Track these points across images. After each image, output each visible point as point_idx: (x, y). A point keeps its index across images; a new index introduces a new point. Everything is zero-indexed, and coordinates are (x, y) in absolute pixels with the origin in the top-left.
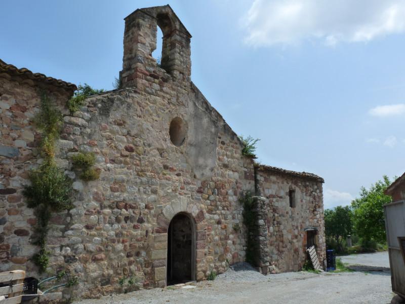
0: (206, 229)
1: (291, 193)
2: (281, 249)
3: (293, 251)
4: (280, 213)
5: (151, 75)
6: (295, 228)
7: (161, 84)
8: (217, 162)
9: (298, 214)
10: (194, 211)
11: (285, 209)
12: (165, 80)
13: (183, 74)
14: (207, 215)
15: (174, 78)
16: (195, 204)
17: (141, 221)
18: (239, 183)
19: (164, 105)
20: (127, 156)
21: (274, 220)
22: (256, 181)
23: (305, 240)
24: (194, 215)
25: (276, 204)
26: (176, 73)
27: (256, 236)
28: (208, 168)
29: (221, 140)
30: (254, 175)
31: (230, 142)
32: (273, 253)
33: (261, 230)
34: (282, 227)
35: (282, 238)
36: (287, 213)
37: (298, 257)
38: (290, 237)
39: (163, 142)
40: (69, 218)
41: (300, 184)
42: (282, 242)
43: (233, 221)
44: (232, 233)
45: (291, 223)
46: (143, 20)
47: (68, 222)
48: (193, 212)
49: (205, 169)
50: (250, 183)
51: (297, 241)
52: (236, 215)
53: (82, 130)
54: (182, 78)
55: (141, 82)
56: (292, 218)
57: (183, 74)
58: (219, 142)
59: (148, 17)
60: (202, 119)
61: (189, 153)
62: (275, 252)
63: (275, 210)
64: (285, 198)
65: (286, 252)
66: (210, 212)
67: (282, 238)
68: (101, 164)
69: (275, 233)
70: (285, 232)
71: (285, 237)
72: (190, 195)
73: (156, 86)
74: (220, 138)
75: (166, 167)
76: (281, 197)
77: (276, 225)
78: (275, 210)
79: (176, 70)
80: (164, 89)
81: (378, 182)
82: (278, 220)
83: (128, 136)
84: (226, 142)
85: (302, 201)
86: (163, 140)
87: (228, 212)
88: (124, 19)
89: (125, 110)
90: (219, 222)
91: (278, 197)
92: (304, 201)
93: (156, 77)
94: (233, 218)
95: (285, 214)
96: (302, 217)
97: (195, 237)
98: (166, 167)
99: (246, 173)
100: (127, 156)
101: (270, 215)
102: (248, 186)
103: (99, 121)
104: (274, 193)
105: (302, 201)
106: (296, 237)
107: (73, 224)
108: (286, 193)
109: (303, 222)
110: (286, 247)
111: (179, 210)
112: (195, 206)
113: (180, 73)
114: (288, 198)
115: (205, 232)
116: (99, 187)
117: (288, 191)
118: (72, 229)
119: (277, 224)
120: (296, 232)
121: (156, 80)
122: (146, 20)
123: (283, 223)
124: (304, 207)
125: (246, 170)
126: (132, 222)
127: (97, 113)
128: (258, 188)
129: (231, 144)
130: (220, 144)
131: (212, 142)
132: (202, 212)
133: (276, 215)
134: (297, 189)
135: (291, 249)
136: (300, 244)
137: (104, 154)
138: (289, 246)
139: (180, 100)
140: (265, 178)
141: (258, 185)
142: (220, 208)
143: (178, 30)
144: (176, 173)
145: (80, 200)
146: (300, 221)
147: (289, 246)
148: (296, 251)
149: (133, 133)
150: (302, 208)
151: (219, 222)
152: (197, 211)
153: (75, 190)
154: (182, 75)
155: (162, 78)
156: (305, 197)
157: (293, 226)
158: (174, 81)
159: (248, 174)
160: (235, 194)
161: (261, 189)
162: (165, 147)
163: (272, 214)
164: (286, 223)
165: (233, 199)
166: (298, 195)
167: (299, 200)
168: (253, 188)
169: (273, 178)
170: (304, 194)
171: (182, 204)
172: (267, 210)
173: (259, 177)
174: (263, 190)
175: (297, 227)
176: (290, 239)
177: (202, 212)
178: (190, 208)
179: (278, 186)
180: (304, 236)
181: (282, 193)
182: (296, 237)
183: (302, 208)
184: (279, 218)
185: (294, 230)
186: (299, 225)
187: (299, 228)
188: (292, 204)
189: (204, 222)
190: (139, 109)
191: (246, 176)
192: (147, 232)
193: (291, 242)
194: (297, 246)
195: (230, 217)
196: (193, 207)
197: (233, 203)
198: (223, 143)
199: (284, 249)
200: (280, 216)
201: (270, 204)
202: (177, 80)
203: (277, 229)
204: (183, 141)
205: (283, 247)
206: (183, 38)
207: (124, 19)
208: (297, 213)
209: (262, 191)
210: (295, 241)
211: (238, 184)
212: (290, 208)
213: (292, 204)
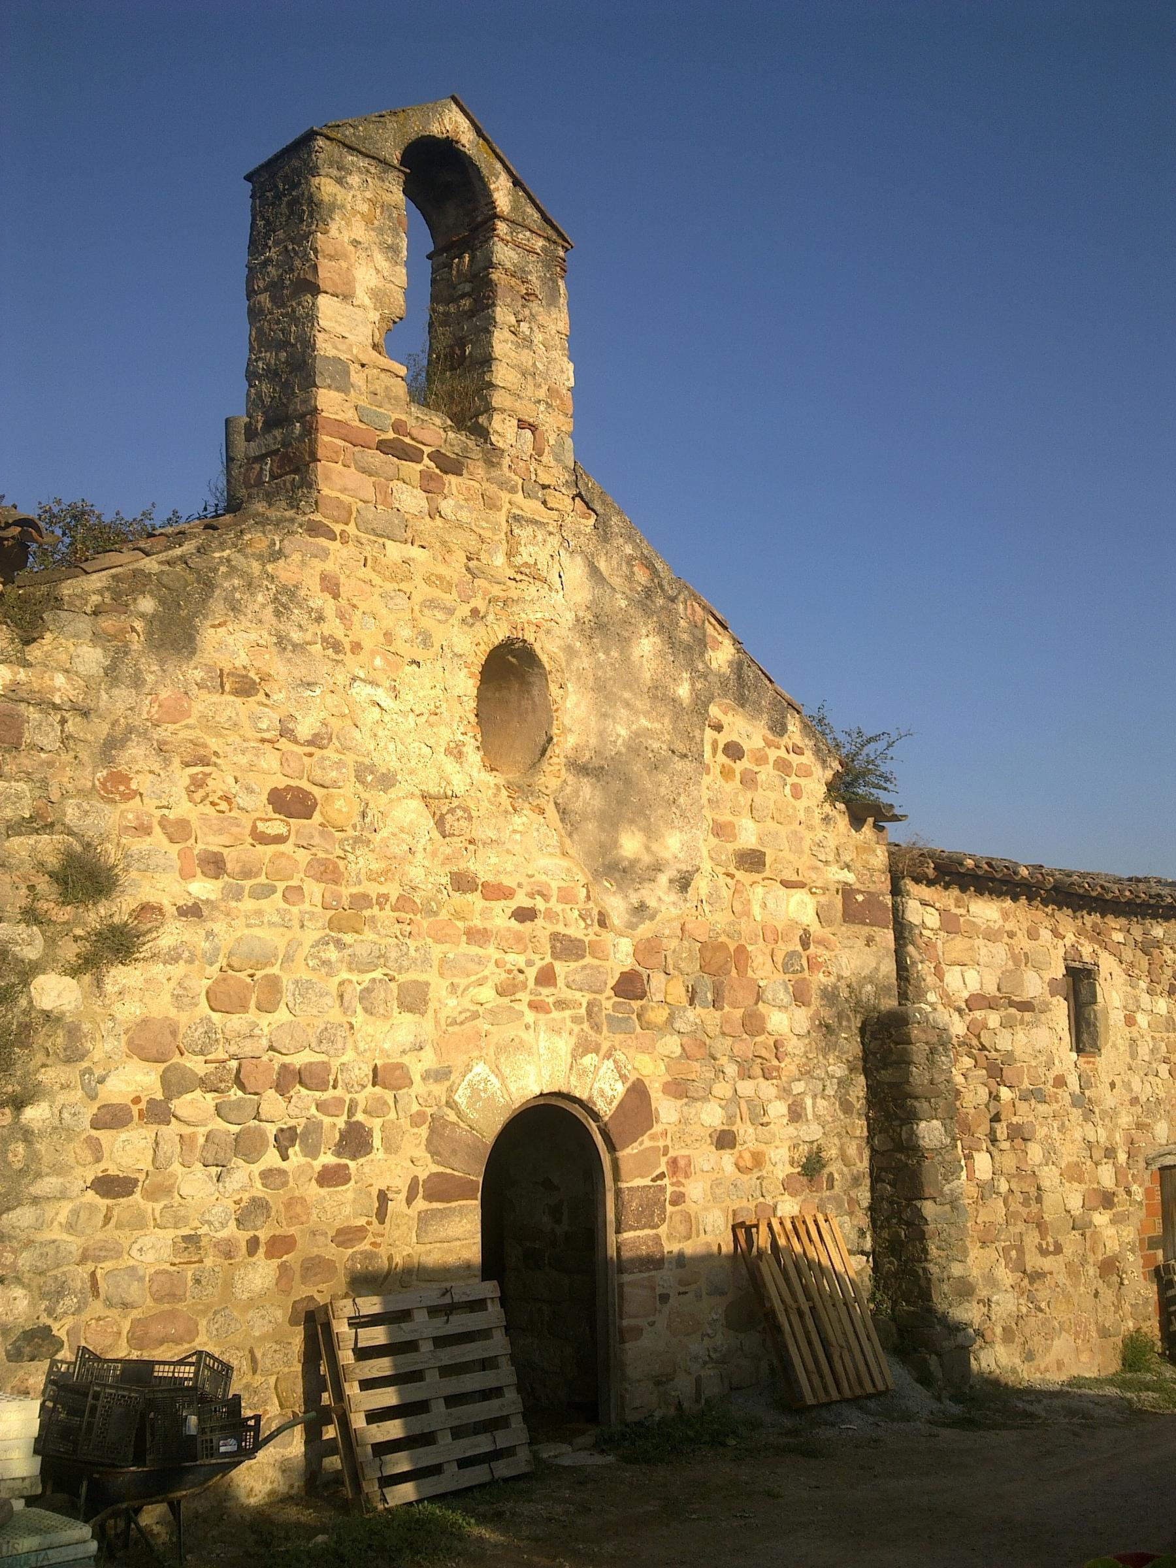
0: (662, 1176)
1: (1079, 983)
2: (1034, 1261)
3: (1092, 1271)
4: (1026, 1085)
5: (384, 447)
6: (1098, 1154)
7: (429, 484)
8: (706, 843)
9: (1113, 1085)
10: (602, 1087)
11: (1049, 1065)
12: (450, 465)
13: (533, 428)
14: (667, 1110)
15: (492, 456)
16: (608, 1056)
17: (355, 1141)
18: (820, 942)
19: (448, 587)
20: (280, 839)
21: (996, 1118)
22: (902, 931)
23: (1149, 1214)
24: (605, 1109)
25: (1004, 1041)
26: (503, 430)
27: (909, 1200)
28: (663, 879)
29: (723, 739)
30: (888, 900)
31: (769, 744)
32: (991, 1281)
33: (931, 1170)
34: (1035, 1152)
35: (1035, 1208)
36: (1060, 1082)
37: (1119, 1297)
38: (1075, 1203)
39: (450, 766)
40: (21, 1148)
41: (1118, 937)
42: (1041, 1226)
43: (791, 1130)
44: (787, 1186)
45: (1077, 1134)
46: (340, 181)
47: (18, 1166)
48: (602, 1093)
49: (652, 880)
50: (869, 941)
51: (1113, 1222)
52: (809, 1102)
53: (70, 727)
54: (529, 448)
55: (339, 478)
56: (1084, 1104)
57: (533, 428)
58: (715, 745)
59: (363, 163)
60: (628, 640)
61: (571, 807)
62: (1006, 1277)
63: (996, 1072)
64: (1046, 1008)
65: (1062, 1278)
66: (678, 1089)
67: (1035, 1208)
68: (156, 880)
69: (1003, 1187)
70: (1049, 1177)
71: (1049, 1199)
72: (583, 1011)
73: (411, 499)
74: (718, 728)
75: (463, 882)
76: (1026, 1006)
77: (1006, 1145)
78: (996, 1072)
79: (503, 411)
80: (447, 506)
81: (384, 1188)
82: (1015, 1120)
83: (284, 743)
84: (746, 745)
85: (1130, 1021)
86: (448, 752)
87: (768, 1089)
88: (248, 178)
89: (268, 613)
90: (725, 1140)
91: (1012, 1004)
92: (1142, 1020)
93: (409, 454)
94: (796, 1114)
95: (1049, 1089)
96: (1135, 1101)
97: (611, 1215)
98: (463, 882)
99: (847, 892)
100: (280, 839)
101: (974, 1095)
102: (860, 959)
103: (150, 678)
104: (991, 989)
105: (1130, 1021)
106: (1107, 1200)
107: (39, 1175)
108: (1053, 982)
109: (1139, 1126)
110: (1058, 1249)
111: (529, 1081)
112: (610, 1064)
113: (522, 424)
114: (1060, 1009)
115: (662, 1189)
116: (138, 991)
117: (1059, 972)
118: (35, 1200)
119: (1010, 1138)
120: (1106, 1176)
121: (412, 469)
122: (354, 180)
123: (1041, 1132)
124: (1144, 1051)
125: (850, 877)
126: (251, 1157)
127: (136, 643)
128: (914, 963)
129: (773, 754)
130: (722, 758)
131: (681, 747)
132: (638, 1092)
133: (1005, 1093)
134: (1107, 964)
135: (1084, 1262)
136: (1129, 1233)
137: (178, 831)
138: (1071, 1242)
139: (526, 554)
140: (943, 913)
141: (911, 948)
142: (731, 1070)
143: (505, 219)
144: (513, 904)
145: (68, 1061)
146: (1125, 1120)
147: (1071, 1242)
148: (1110, 1267)
149: (305, 728)
150: (1134, 1055)
151: (725, 1140)
152: (620, 1089)
153: (47, 1015)
154: (528, 433)
155: (436, 456)
156: (1145, 999)
157: (1090, 1146)
158: (491, 464)
159: (860, 898)
160: (800, 997)
161: (925, 969)
162: (459, 784)
163: (983, 1092)
164: (1055, 1134)
165: (786, 1022)
166: (1113, 992)
167: (1116, 1017)
168: (888, 967)
169: (986, 911)
170: (1143, 985)
171: (539, 1064)
172: (963, 1072)
173: (914, 912)
174: (939, 973)
175: (1110, 1153)
176: (1077, 1211)
177: (638, 1092)
178: (583, 1073)
179: (1011, 947)
180: (1148, 1193)
181: (1033, 986)
182: (1107, 1200)
183: (1134, 1055)
184: (1022, 1107)
185: (1097, 1164)
186: (1118, 1137)
187: (1122, 1157)
188: (1084, 1032)
189: (652, 1138)
190: (329, 607)
191: (853, 909)
192: (383, 1197)
193: (1080, 1226)
194: (1113, 1247)
195: (777, 1109)
196: (597, 1068)
197: (794, 1046)
198: (734, 751)
199: (1047, 1263)
200: (1024, 1099)
201: (975, 1042)
202: (506, 461)
203: (1009, 1162)
204: (544, 752)
205: (1044, 1252)
206: (532, 251)
207: (248, 178)
208: (1107, 1081)
209: (930, 980)
210: (1101, 1218)
211: (812, 949)
212: (1074, 1055)
213: (1084, 1032)
